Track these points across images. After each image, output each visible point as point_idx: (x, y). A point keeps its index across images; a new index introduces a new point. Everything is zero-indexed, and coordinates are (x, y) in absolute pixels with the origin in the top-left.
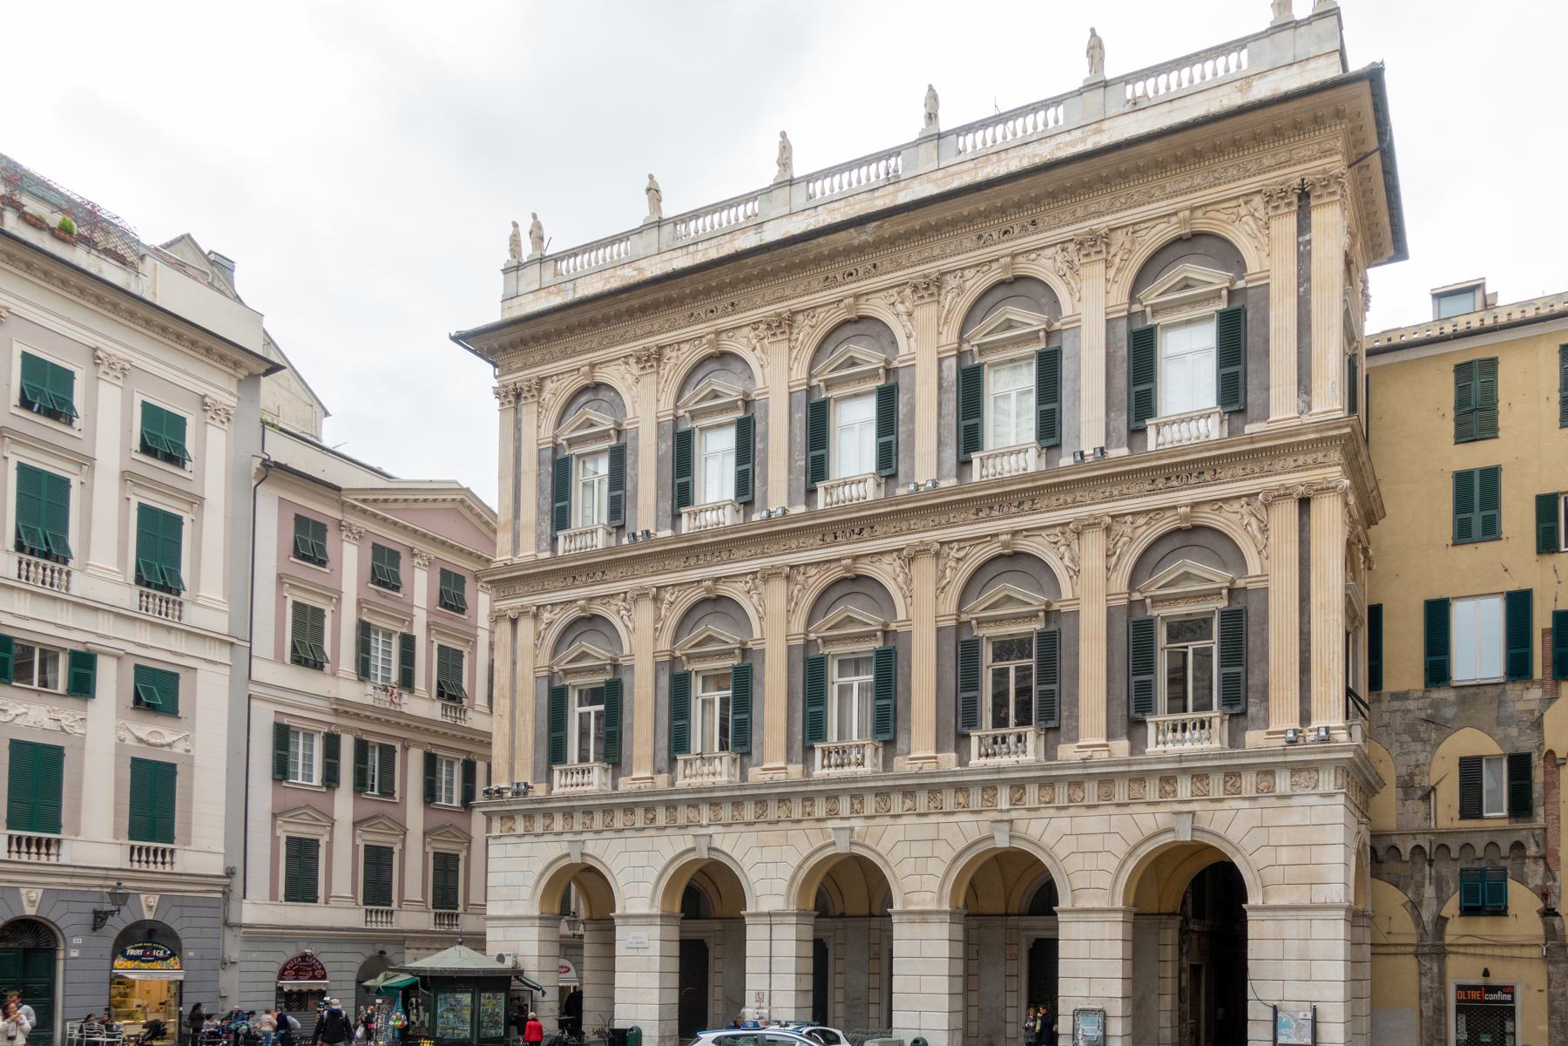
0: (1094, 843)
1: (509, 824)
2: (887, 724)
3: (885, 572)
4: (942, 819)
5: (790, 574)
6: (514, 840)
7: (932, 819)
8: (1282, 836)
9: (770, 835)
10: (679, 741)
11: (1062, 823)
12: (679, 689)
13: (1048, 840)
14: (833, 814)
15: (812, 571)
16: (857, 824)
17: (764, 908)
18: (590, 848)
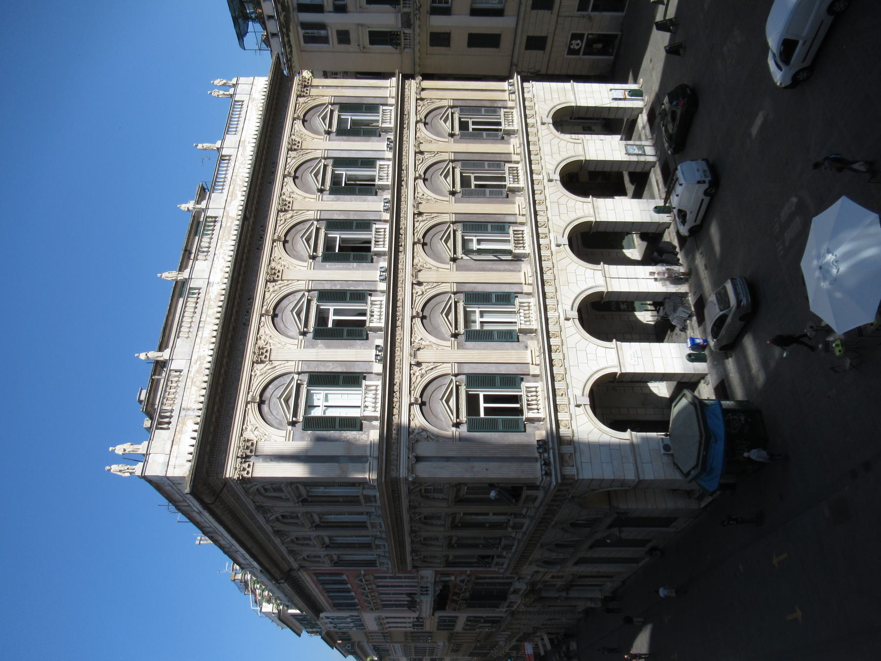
0: (555, 149)
1: (567, 458)
2: (500, 226)
3: (422, 227)
4: (548, 201)
5: (417, 271)
6: (578, 455)
7: (548, 205)
8: (548, 96)
9: (561, 279)
10: (509, 336)
11: (547, 158)
12: (474, 336)
13: (556, 163)
14: (549, 247)
15: (416, 261)
16: (552, 236)
17: (602, 282)
18: (579, 393)
